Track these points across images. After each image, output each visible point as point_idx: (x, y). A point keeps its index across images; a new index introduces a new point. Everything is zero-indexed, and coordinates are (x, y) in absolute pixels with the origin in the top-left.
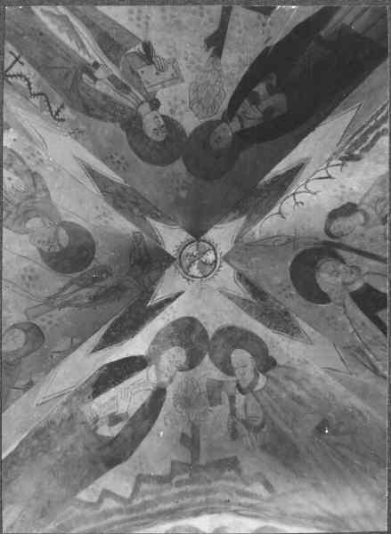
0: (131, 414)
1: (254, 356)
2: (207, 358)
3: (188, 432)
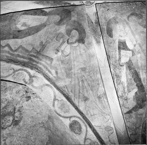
0: (31, 26)
1: (80, 37)
2: (65, 25)
3: (44, 42)
